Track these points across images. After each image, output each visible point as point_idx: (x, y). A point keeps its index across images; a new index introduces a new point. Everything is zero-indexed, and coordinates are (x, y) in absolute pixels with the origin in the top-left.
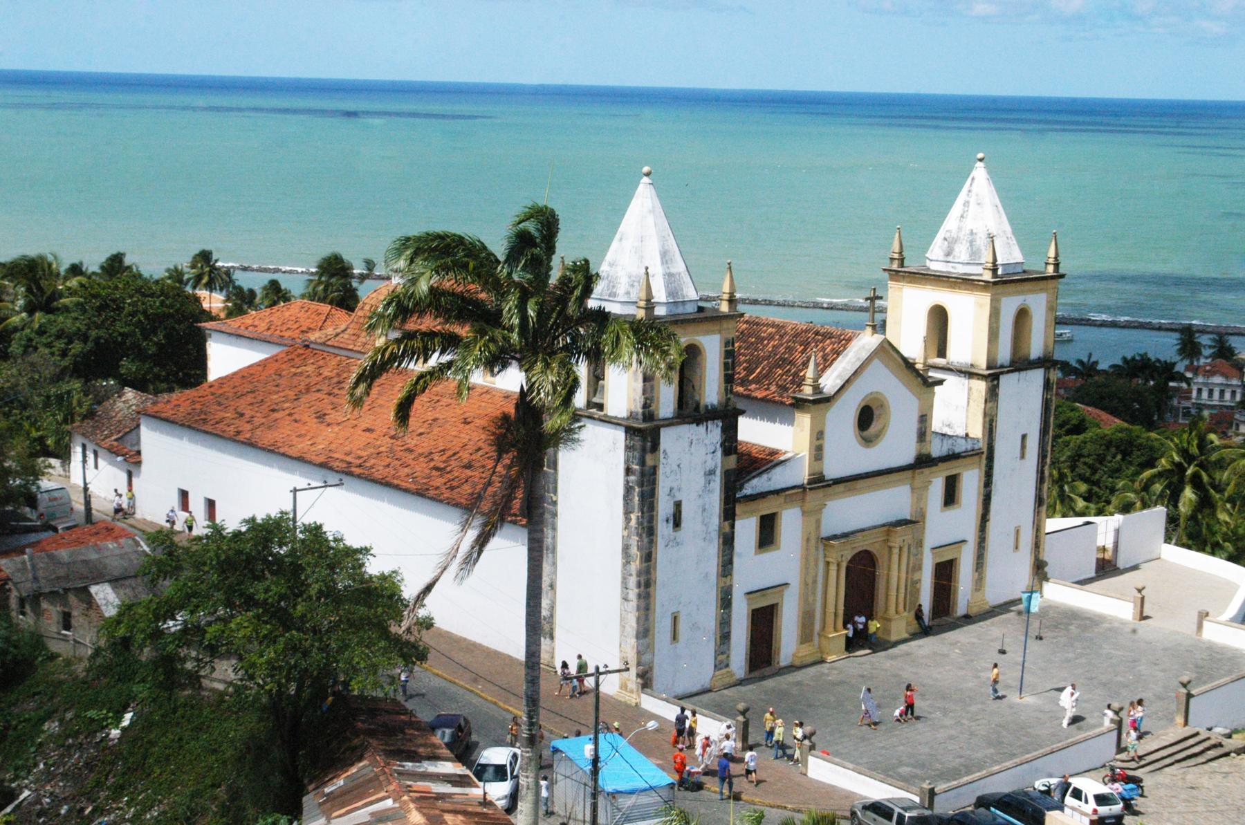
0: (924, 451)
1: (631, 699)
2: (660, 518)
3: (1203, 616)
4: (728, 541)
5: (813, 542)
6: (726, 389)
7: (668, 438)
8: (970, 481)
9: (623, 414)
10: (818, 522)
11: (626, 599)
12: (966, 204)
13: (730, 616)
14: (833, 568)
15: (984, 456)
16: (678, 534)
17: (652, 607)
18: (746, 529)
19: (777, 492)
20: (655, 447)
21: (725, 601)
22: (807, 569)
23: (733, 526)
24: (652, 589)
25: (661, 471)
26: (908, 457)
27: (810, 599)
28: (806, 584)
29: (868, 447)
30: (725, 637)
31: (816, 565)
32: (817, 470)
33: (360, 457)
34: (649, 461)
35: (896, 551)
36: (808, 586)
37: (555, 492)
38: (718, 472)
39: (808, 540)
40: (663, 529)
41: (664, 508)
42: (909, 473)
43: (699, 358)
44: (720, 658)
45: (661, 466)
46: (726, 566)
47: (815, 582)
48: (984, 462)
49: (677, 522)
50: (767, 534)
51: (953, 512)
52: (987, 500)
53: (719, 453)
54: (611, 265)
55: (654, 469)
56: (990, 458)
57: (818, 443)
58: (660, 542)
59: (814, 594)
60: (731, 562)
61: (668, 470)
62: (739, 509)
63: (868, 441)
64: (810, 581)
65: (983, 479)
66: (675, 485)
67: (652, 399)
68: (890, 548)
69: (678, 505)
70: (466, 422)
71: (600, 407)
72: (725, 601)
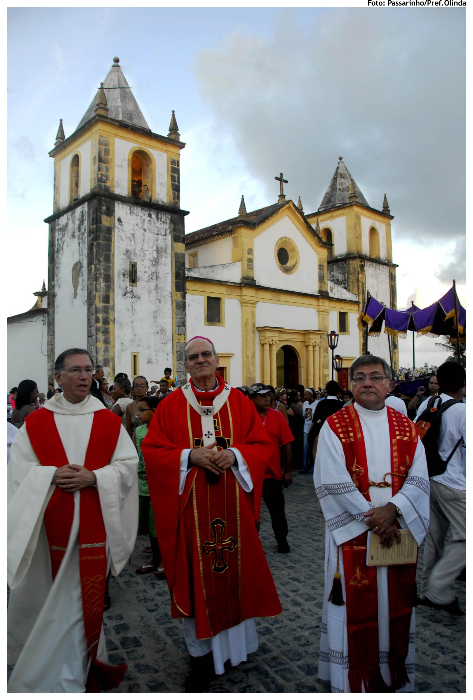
0: (323, 289)
2: (116, 272)
4: (181, 307)
5: (250, 327)
6: (174, 194)
7: (121, 210)
10: (253, 314)
14: (267, 347)
16: (134, 288)
17: (111, 340)
18: (196, 303)
19: (220, 283)
20: (110, 212)
22: (247, 345)
23: (184, 297)
24: (110, 327)
25: (116, 234)
26: (314, 289)
27: (252, 369)
28: (247, 357)
31: (254, 345)
32: (250, 274)
34: (105, 221)
35: (311, 348)
38: (169, 251)
39: (246, 324)
40: (120, 283)
41: (119, 264)
42: (313, 302)
43: (148, 165)
45: (116, 230)
47: (254, 357)
49: (133, 278)
53: (169, 238)
55: (109, 230)
57: (250, 256)
59: (253, 365)
61: (123, 234)
62: (188, 285)
63: (287, 271)
64: (250, 355)
66: (129, 248)
67: (107, 177)
68: (307, 346)
69: (134, 266)
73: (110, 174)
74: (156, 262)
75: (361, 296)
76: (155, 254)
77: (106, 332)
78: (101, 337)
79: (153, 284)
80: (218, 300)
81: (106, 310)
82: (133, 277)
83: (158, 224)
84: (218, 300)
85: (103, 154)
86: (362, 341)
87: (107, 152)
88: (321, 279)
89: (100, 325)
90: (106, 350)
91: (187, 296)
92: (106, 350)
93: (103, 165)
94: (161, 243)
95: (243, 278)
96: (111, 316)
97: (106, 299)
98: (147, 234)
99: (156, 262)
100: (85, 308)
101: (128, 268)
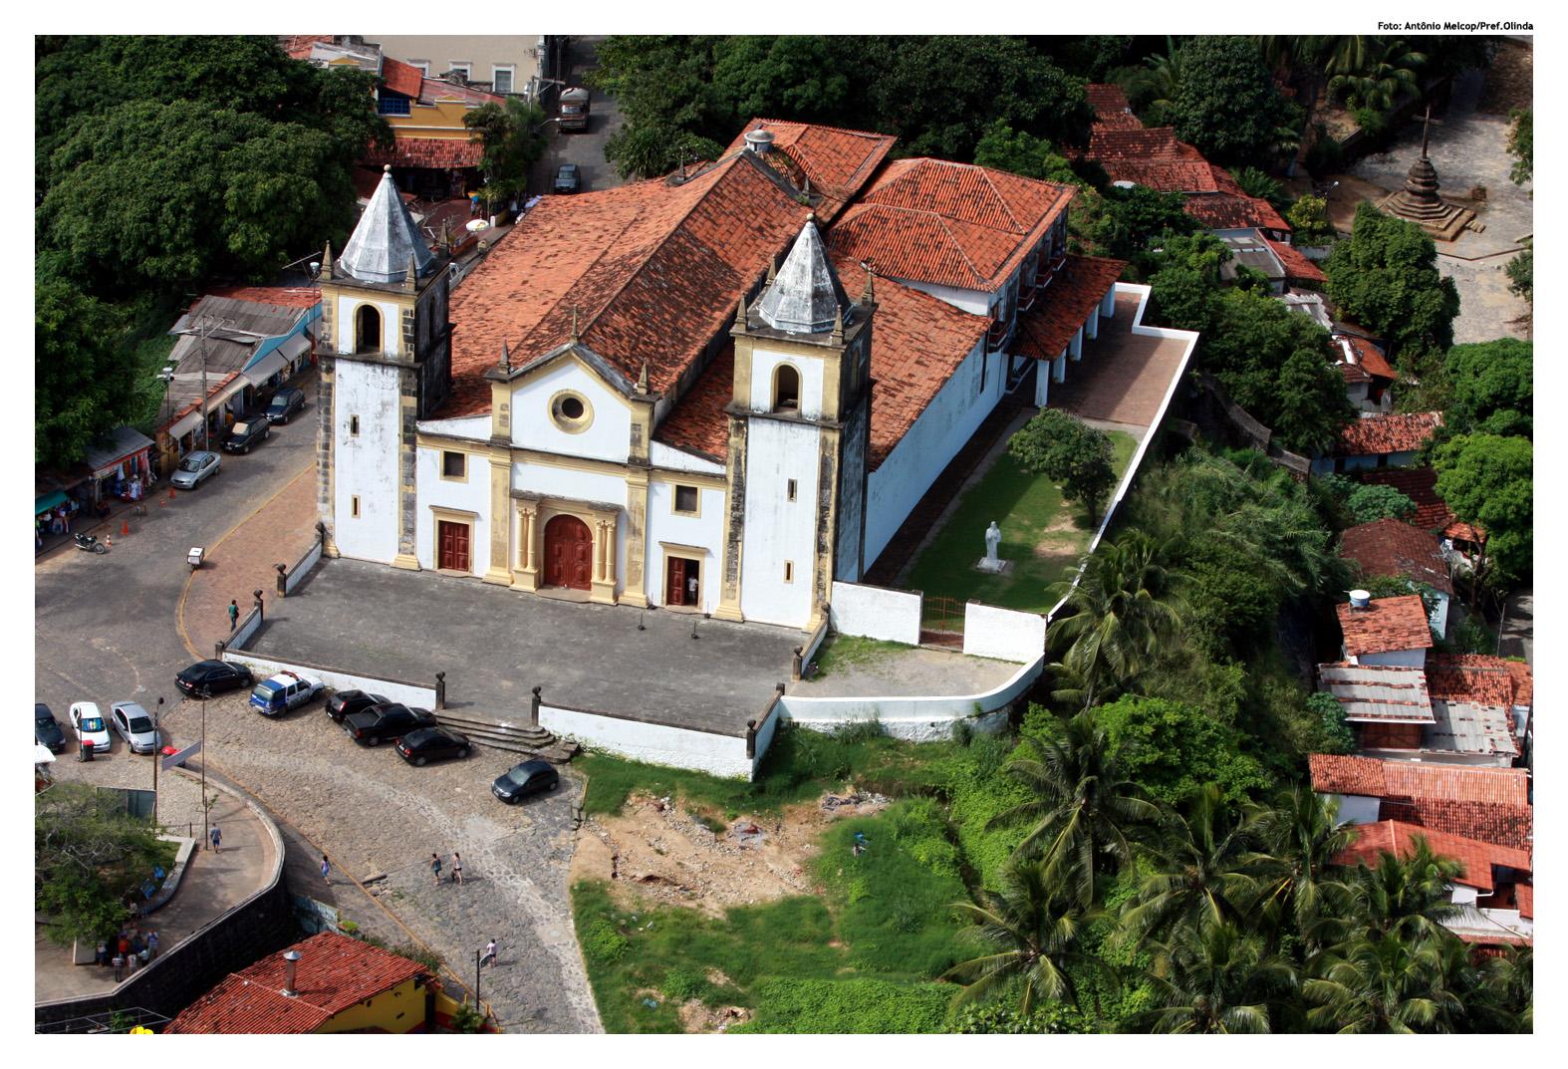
0: (639, 455)
4: (411, 460)
7: (341, 367)
13: (414, 515)
15: (731, 479)
18: (430, 459)
21: (409, 505)
23: (414, 450)
24: (330, 470)
26: (622, 454)
28: (494, 519)
29: (566, 428)
30: (409, 530)
32: (505, 432)
36: (502, 524)
38: (397, 404)
39: (494, 486)
40: (341, 431)
44: (405, 545)
46: (410, 477)
48: (731, 488)
50: (453, 466)
52: (738, 523)
53: (397, 392)
55: (330, 386)
60: (413, 476)
62: (419, 440)
65: (730, 503)
72: (409, 505)
73: (334, 332)
74: (380, 415)
75: (732, 468)
76: (380, 408)
77: (326, 474)
78: (321, 478)
79: (376, 436)
80: (461, 456)
81: (326, 456)
82: (355, 427)
83: (384, 378)
84: (461, 456)
85: (325, 315)
86: (729, 529)
87: (330, 311)
88: (635, 441)
89: (320, 467)
90: (326, 490)
91: (419, 451)
92: (326, 490)
93: (326, 325)
94: (387, 398)
95: (494, 437)
96: (330, 461)
97: (326, 447)
98: (371, 388)
99: (380, 415)
101: (350, 420)
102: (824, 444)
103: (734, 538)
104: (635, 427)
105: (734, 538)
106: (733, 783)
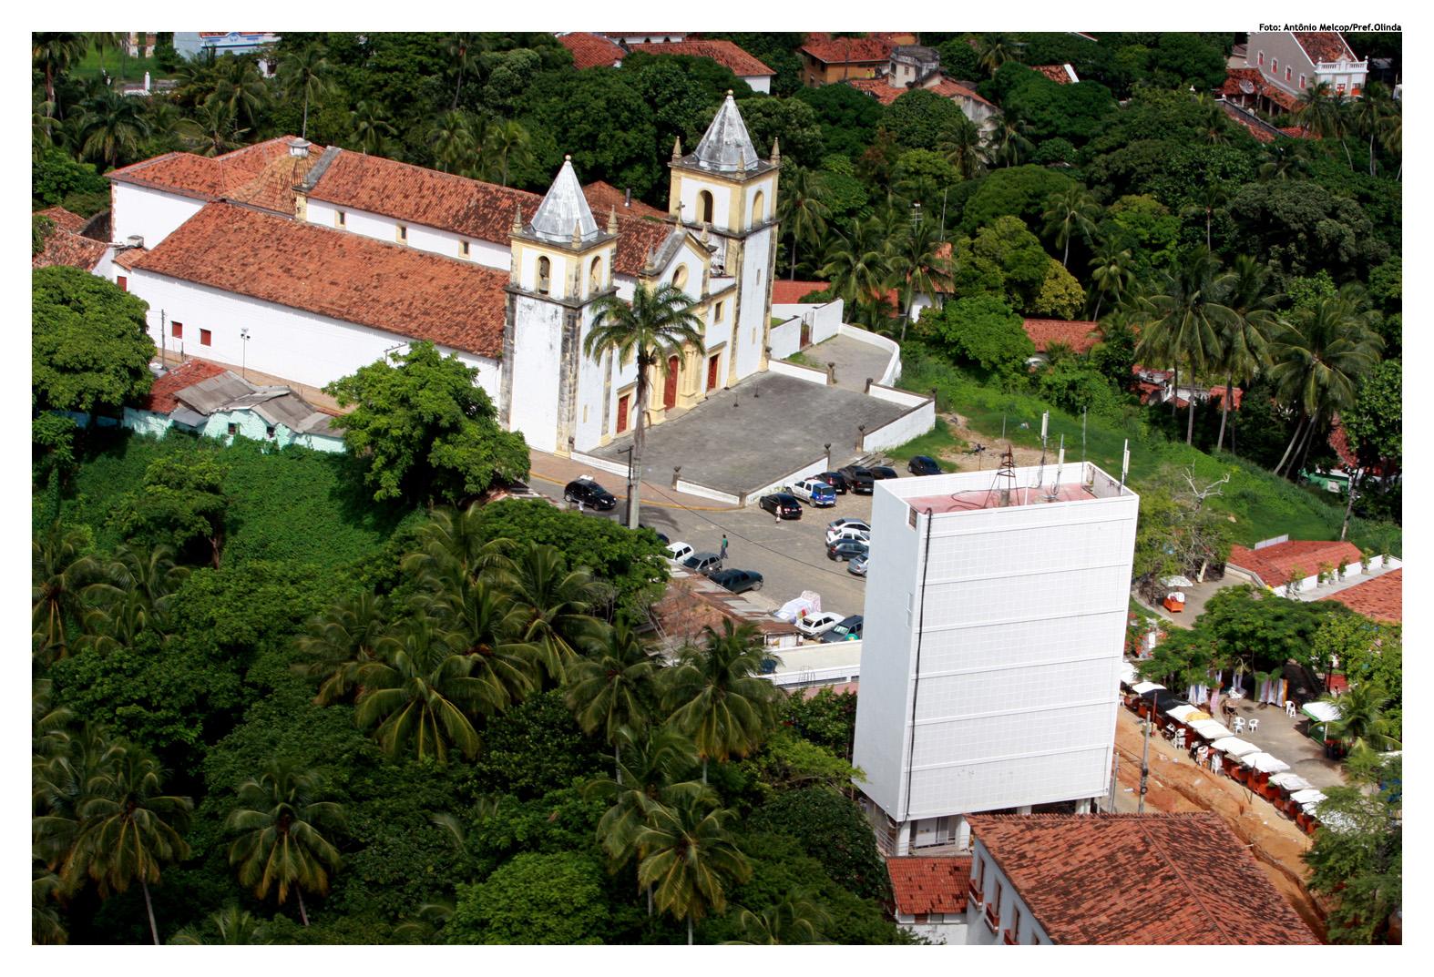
1: (565, 455)
3: (869, 382)
8: (729, 303)
9: (562, 297)
11: (561, 399)
12: (722, 124)
33: (343, 307)
37: (513, 338)
51: (720, 325)
54: (551, 212)
56: (740, 288)
58: (580, 366)
70: (403, 277)
71: (546, 292)
72: (608, 396)
88: (704, 283)
97: (575, 376)
100: (558, 378)
102: (772, 236)
103: (736, 326)
104: (705, 272)
105: (736, 326)
106: (931, 435)
